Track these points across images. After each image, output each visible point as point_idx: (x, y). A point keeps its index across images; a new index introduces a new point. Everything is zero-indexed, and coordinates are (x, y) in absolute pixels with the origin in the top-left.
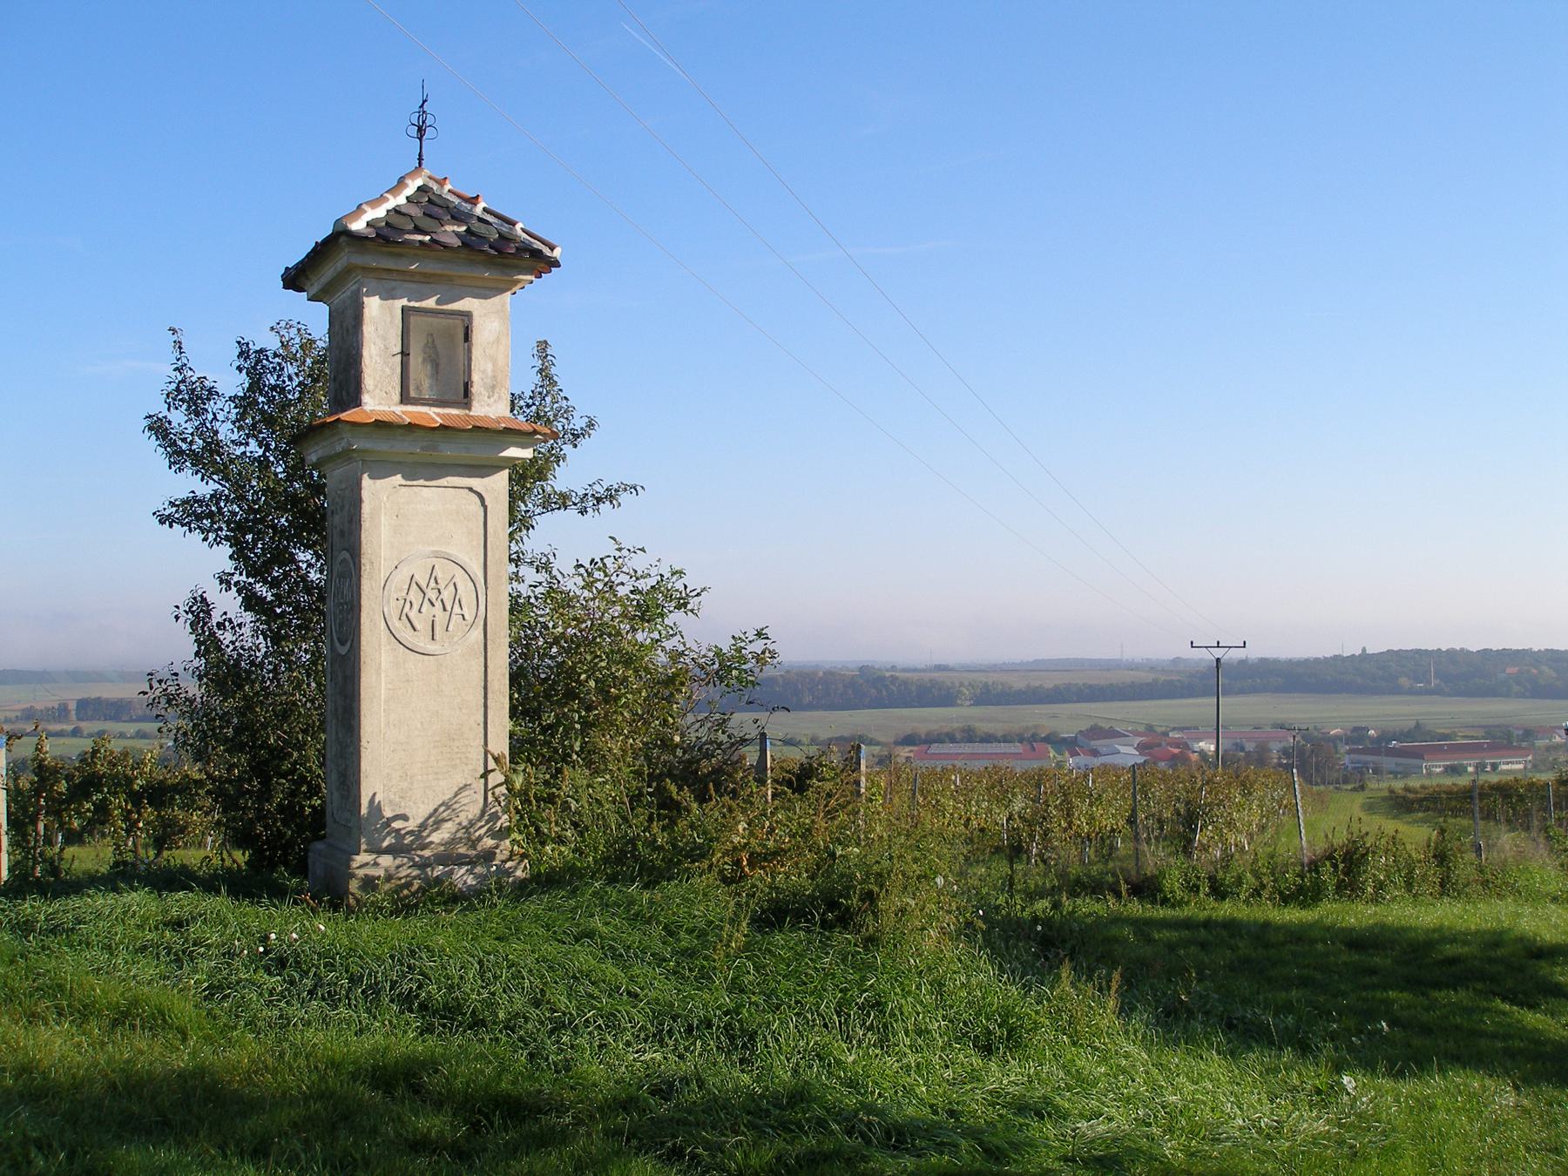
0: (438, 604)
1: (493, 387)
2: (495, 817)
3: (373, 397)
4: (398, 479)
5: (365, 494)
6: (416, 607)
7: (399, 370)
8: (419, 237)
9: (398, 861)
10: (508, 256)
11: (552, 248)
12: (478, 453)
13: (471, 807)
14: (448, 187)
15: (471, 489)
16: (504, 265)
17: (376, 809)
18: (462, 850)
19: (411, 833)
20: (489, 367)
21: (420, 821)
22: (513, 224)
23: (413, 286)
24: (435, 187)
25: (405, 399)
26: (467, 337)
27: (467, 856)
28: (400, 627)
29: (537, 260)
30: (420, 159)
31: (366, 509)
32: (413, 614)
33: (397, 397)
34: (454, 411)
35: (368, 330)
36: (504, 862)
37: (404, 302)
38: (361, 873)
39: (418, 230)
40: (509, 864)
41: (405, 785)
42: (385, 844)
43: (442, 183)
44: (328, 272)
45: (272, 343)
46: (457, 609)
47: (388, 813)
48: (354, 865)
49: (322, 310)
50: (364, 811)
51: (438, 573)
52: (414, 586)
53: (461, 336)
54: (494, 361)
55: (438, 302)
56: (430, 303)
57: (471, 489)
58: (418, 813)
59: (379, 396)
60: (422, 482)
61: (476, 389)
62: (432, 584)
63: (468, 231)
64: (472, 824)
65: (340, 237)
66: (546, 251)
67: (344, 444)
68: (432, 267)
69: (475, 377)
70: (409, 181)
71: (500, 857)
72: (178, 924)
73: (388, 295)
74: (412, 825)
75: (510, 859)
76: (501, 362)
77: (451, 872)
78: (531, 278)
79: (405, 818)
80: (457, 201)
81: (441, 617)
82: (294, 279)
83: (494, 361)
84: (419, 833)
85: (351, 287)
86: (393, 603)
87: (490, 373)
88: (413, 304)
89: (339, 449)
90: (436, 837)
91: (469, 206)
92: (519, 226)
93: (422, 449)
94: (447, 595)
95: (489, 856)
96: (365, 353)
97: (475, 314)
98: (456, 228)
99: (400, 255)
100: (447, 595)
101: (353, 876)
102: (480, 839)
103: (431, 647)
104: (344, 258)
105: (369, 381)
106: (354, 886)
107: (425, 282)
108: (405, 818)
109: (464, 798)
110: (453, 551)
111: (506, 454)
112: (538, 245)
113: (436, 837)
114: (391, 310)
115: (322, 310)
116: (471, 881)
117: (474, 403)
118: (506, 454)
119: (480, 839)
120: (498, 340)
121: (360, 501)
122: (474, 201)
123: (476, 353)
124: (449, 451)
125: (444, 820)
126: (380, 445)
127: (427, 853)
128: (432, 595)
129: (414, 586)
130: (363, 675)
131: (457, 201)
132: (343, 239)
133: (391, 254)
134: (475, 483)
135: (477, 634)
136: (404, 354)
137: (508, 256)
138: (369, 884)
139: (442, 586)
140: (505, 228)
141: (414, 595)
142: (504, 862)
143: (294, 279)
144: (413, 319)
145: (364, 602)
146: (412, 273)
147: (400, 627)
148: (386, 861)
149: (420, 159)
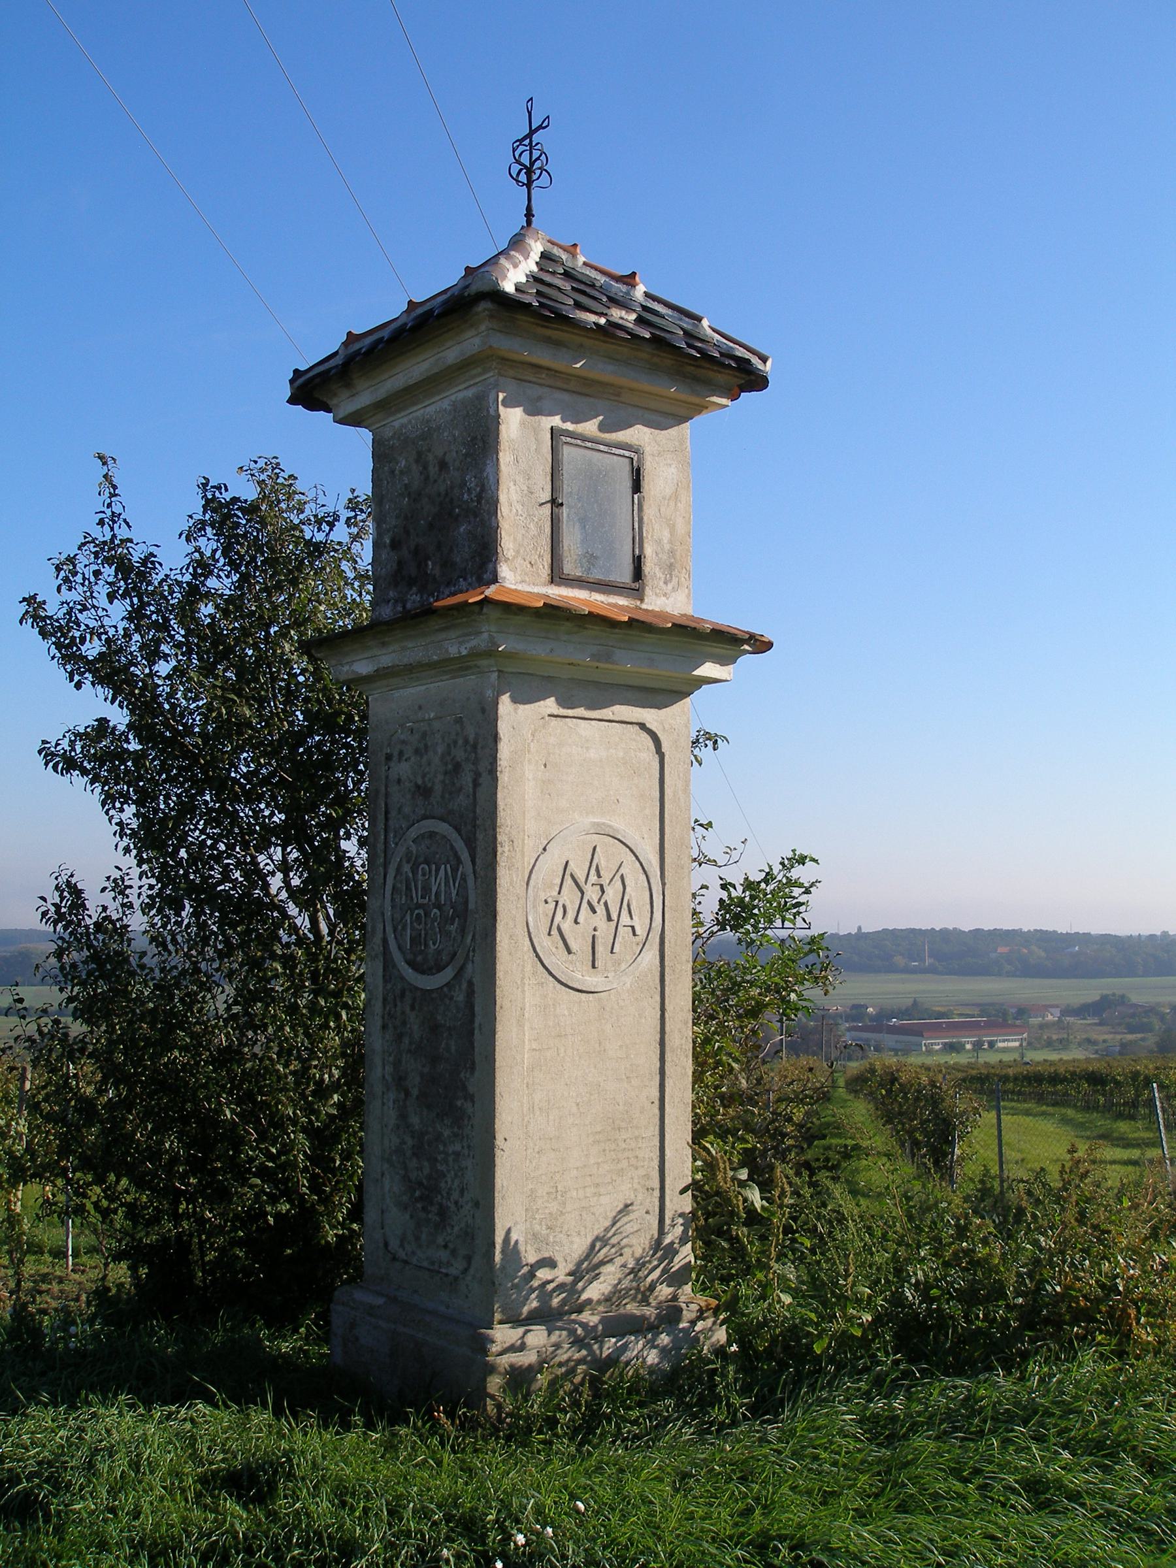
0: (600, 909)
1: (671, 566)
2: (671, 1252)
3: (514, 570)
4: (550, 705)
5: (503, 728)
6: (571, 915)
7: (548, 530)
8: (592, 318)
9: (554, 1338)
10: (699, 368)
11: (764, 360)
12: (663, 670)
13: (638, 1238)
14: (581, 259)
15: (642, 726)
16: (697, 380)
17: (512, 1252)
18: (632, 1308)
19: (561, 1287)
20: (666, 535)
21: (571, 1267)
22: (699, 319)
23: (566, 397)
24: (564, 256)
25: (557, 576)
26: (637, 487)
27: (643, 1318)
28: (548, 945)
29: (745, 376)
30: (529, 215)
31: (505, 751)
32: (567, 926)
33: (545, 572)
34: (622, 601)
35: (505, 458)
36: (693, 1323)
37: (556, 421)
38: (505, 1361)
39: (578, 305)
40: (700, 1326)
41: (554, 1207)
42: (525, 1310)
43: (572, 250)
44: (415, 367)
45: (248, 492)
46: (625, 919)
47: (531, 1257)
48: (495, 1349)
49: (361, 440)
50: (498, 1257)
51: (600, 858)
52: (568, 877)
53: (627, 484)
54: (672, 529)
55: (602, 428)
56: (590, 427)
57: (642, 726)
58: (570, 1249)
59: (520, 574)
60: (581, 712)
61: (648, 567)
62: (593, 878)
63: (640, 320)
64: (640, 1264)
65: (470, 301)
66: (755, 361)
67: (480, 642)
68: (605, 372)
69: (649, 550)
70: (531, 242)
71: (688, 1314)
72: (251, 1482)
73: (534, 410)
74: (561, 1274)
75: (700, 1317)
76: (681, 528)
77: (625, 1347)
78: (724, 401)
79: (550, 1263)
80: (602, 279)
81: (605, 930)
82: (310, 390)
83: (672, 529)
84: (570, 1289)
85: (461, 393)
86: (542, 907)
87: (667, 547)
88: (569, 426)
89: (455, 648)
90: (594, 1291)
91: (624, 288)
92: (705, 323)
93: (594, 657)
94: (612, 895)
95: (671, 1314)
96: (503, 497)
97: (648, 450)
98: (623, 313)
99: (558, 344)
100: (612, 895)
101: (491, 1369)
102: (652, 1288)
103: (591, 980)
104: (468, 342)
105: (508, 543)
106: (494, 1384)
107: (580, 395)
108: (550, 1263)
109: (629, 1225)
110: (619, 824)
111: (698, 672)
112: (740, 352)
113: (594, 1291)
114: (536, 431)
115: (361, 440)
116: (652, 1357)
117: (648, 591)
118: (698, 672)
119: (652, 1288)
120: (675, 496)
121: (495, 738)
122: (629, 280)
123: (649, 512)
124: (630, 664)
125: (602, 1263)
126: (539, 649)
127: (590, 1318)
128: (592, 894)
129: (568, 881)
130: (499, 1027)
131: (602, 279)
132: (484, 306)
133: (548, 341)
134: (649, 716)
135: (650, 956)
136: (555, 503)
137: (699, 368)
138: (519, 1379)
139: (605, 881)
140: (687, 324)
141: (569, 896)
142: (693, 1323)
143: (310, 390)
144: (568, 453)
145: (501, 906)
146: (568, 377)
147: (548, 945)
148: (538, 1337)
149: (529, 215)
